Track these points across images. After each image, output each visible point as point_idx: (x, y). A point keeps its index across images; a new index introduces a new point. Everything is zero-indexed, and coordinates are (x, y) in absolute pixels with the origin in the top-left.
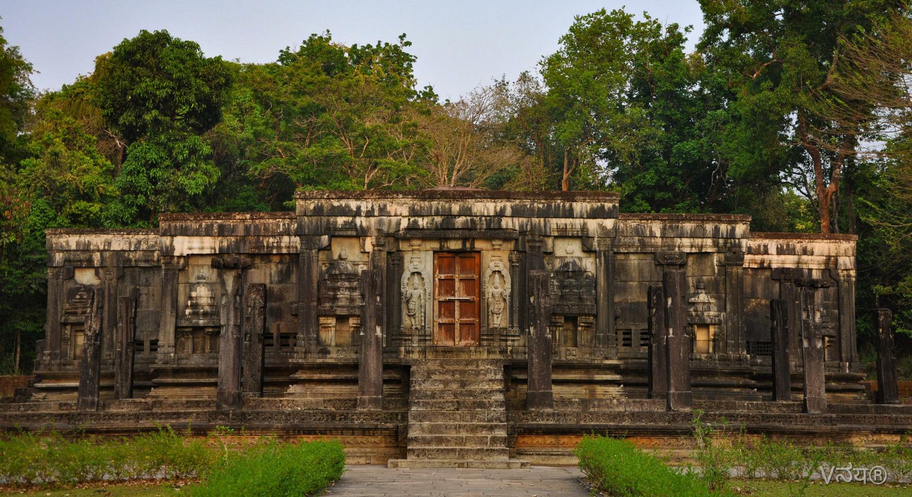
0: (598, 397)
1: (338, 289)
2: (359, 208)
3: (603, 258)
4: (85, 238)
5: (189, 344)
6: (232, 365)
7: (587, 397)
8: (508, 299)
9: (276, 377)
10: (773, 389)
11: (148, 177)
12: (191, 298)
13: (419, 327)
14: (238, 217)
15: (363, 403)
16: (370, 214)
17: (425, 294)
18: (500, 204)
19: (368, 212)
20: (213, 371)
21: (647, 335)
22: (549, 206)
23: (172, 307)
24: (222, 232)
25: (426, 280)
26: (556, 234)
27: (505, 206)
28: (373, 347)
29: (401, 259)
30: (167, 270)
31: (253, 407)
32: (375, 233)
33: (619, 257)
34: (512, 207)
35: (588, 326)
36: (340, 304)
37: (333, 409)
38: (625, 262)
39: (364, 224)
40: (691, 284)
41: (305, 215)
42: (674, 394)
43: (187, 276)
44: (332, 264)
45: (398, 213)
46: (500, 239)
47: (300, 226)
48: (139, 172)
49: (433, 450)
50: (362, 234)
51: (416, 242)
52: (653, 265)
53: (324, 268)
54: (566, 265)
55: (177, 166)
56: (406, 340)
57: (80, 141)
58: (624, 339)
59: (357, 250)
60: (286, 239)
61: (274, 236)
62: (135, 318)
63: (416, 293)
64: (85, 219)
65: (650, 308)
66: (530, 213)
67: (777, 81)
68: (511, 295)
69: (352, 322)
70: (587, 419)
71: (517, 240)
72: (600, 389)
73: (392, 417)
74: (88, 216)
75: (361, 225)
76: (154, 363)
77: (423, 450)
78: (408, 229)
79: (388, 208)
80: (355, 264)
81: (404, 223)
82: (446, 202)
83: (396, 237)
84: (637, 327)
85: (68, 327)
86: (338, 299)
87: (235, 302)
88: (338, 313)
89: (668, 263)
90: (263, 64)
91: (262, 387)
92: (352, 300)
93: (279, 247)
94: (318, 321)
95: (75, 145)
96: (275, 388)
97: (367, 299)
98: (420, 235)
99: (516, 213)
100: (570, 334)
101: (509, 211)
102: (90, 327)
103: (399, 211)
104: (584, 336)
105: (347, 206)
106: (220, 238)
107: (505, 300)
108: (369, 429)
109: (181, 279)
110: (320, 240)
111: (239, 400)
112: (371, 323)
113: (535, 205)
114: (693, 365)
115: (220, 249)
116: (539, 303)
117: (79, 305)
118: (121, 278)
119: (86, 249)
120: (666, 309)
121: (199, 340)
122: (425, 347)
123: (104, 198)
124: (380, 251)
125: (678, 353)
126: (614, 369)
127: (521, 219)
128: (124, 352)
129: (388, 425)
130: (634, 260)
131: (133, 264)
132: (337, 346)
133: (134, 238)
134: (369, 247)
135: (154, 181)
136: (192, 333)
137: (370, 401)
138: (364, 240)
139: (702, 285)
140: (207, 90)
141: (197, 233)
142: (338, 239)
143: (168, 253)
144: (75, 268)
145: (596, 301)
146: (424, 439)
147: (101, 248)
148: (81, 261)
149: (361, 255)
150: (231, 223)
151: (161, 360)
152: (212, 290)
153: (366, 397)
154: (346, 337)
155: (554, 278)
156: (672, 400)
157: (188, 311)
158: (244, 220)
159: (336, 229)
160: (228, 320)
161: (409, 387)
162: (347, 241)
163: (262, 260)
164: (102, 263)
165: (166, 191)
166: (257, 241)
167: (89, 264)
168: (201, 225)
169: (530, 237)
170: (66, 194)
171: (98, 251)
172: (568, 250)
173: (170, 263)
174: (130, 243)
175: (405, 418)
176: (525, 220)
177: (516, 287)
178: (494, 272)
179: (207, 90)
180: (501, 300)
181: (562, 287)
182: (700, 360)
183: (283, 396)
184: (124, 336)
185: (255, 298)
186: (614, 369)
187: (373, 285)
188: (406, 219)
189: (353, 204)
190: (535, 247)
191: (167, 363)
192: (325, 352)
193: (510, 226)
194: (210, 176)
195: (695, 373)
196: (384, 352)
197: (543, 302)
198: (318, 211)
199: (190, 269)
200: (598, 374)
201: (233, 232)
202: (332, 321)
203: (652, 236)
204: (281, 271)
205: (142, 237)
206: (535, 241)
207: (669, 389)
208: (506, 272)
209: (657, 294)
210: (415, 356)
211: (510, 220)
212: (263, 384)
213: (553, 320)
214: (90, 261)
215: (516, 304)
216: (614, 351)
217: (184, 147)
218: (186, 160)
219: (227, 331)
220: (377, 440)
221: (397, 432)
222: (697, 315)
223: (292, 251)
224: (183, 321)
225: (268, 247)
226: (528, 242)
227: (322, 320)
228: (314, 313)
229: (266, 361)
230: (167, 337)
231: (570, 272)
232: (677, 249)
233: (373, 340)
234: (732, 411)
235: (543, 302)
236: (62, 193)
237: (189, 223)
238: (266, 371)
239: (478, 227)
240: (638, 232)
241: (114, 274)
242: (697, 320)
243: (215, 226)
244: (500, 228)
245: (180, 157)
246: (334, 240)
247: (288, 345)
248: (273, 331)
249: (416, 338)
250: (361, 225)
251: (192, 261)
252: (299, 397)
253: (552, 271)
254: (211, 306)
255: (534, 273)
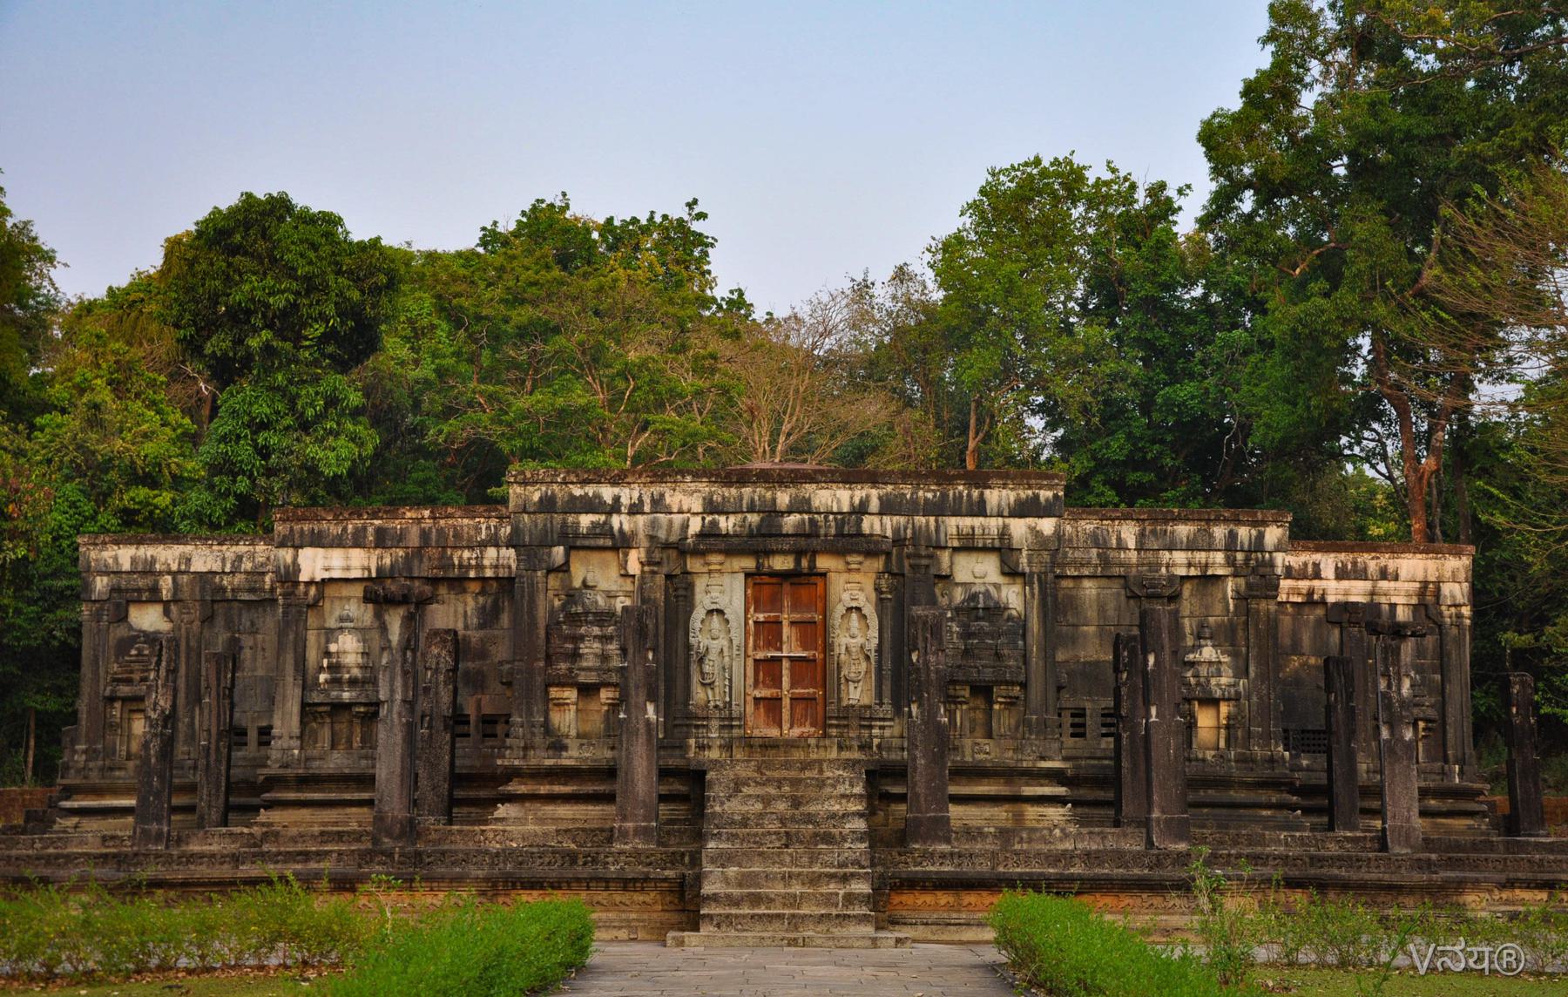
0: (1029, 824)
1: (582, 638)
2: (617, 499)
3: (1036, 586)
4: (146, 551)
5: (326, 733)
6: (398, 770)
7: (1009, 825)
8: (873, 655)
9: (474, 791)
10: (1329, 811)
11: (255, 446)
12: (328, 654)
13: (720, 704)
14: (409, 515)
15: (624, 834)
16: (635, 510)
17: (731, 647)
18: (859, 493)
19: (632, 506)
20: (366, 780)
21: (1113, 719)
22: (944, 496)
23: (296, 670)
24: (382, 540)
25: (733, 624)
26: (956, 544)
27: (868, 496)
28: (642, 739)
29: (690, 587)
30: (287, 606)
31: (434, 842)
32: (645, 543)
33: (1065, 583)
34: (880, 498)
35: (1011, 703)
36: (585, 664)
37: (573, 846)
38: (1074, 592)
39: (626, 527)
40: (1188, 630)
41: (525, 511)
42: (1158, 820)
43: (322, 616)
44: (572, 596)
45: (685, 508)
46: (859, 553)
47: (516, 531)
48: (238, 437)
49: (744, 916)
50: (621, 543)
51: (715, 559)
52: (1123, 598)
53: (557, 603)
54: (974, 597)
55: (305, 426)
56: (697, 727)
57: (138, 384)
58: (1073, 725)
59: (614, 572)
60: (491, 552)
61: (471, 548)
62: (231, 689)
63: (715, 646)
64: (145, 519)
65: (1117, 670)
66: (912, 508)
67: (1335, 280)
68: (879, 650)
69: (605, 695)
70: (1010, 862)
71: (888, 554)
72: (1031, 811)
73: (674, 860)
74: (151, 513)
75: (621, 529)
76: (265, 766)
77: (728, 916)
78: (701, 535)
79: (668, 500)
80: (610, 596)
81: (695, 525)
82: (768, 489)
83: (680, 548)
84: (1096, 704)
85: (118, 705)
86: (581, 656)
87: (405, 661)
88: (581, 679)
89: (1149, 594)
90: (452, 251)
91: (450, 808)
92: (604, 657)
93: (480, 567)
94: (547, 693)
95: (128, 391)
96: (473, 810)
97: (630, 656)
98: (723, 546)
99: (887, 508)
100: (979, 715)
101: (874, 505)
102: (156, 704)
103: (686, 504)
104: (1004, 720)
105: (597, 496)
106: (378, 551)
107: (868, 658)
108: (635, 880)
109: (312, 621)
110: (549, 554)
111: (411, 830)
112: (638, 696)
113: (921, 493)
114: (1191, 769)
115: (379, 569)
116: (926, 663)
117: (136, 666)
118: (208, 619)
119: (148, 570)
120: (1145, 673)
121: (342, 727)
122: (731, 739)
123: (178, 482)
124: (653, 573)
125: (1165, 749)
126: (1056, 776)
127: (895, 518)
128: (213, 747)
129: (667, 873)
130: (1090, 589)
131: (229, 595)
132: (579, 736)
133: (230, 551)
134: (634, 567)
135: (264, 452)
136: (330, 714)
137: (637, 832)
138: (626, 555)
139: (1207, 632)
140: (355, 295)
141: (338, 543)
142: (582, 553)
143: (289, 577)
144: (128, 602)
145: (1025, 658)
146: (728, 897)
147: (174, 567)
148: (139, 590)
149: (621, 580)
150: (397, 525)
151: (276, 761)
152: (365, 641)
153: (630, 825)
154: (596, 722)
155: (952, 619)
156: (1155, 829)
157: (323, 677)
158: (419, 520)
159: (577, 535)
160: (392, 691)
161: (702, 806)
162: (595, 557)
163: (451, 588)
164: (175, 594)
165: (286, 470)
166: (443, 556)
167: (154, 596)
168: (345, 529)
169: (911, 549)
170: (113, 475)
171: (169, 572)
172: (977, 572)
173: (293, 593)
174: (224, 560)
175: (696, 860)
176: (902, 520)
177: (888, 635)
178: (850, 609)
179: (355, 295)
180: (862, 657)
181: (966, 635)
182: (1204, 760)
183: (486, 822)
184: (214, 720)
185: (439, 654)
186: (1056, 776)
187: (642, 632)
188: (699, 518)
189: (607, 493)
190: (919, 566)
191: (286, 766)
192: (558, 747)
193: (877, 530)
194: (361, 445)
195: (1194, 783)
196: (661, 747)
197: (933, 661)
198: (547, 504)
199: (327, 605)
200: (1028, 785)
201: (400, 540)
202: (571, 694)
203: (1121, 547)
204: (484, 607)
205: (245, 549)
206: (920, 556)
207: (1149, 811)
208: (869, 610)
209: (1129, 647)
210: (714, 754)
211: (876, 519)
212: (453, 802)
213: (951, 692)
214: (155, 590)
215: (887, 665)
216: (1056, 745)
217: (317, 393)
218: (321, 417)
219: (390, 711)
220: (647, 899)
221: (682, 885)
222: (1198, 684)
223: (502, 573)
224: (314, 694)
225: (461, 566)
226: (909, 557)
227: (554, 692)
228: (539, 679)
229: (458, 762)
230: (286, 721)
231: (981, 611)
232: (1163, 570)
233: (641, 726)
234: (1259, 849)
235: (933, 661)
236: (107, 473)
237: (325, 525)
238: (457, 779)
239: (822, 532)
240: (1097, 540)
241: (196, 612)
242: (1198, 692)
243: (370, 530)
244: (860, 534)
245: (310, 412)
246: (573, 554)
247: (495, 736)
248: (470, 710)
249: (715, 724)
250: (621, 529)
251: (330, 591)
252: (515, 825)
253: (949, 607)
254: (363, 667)
255: (918, 611)
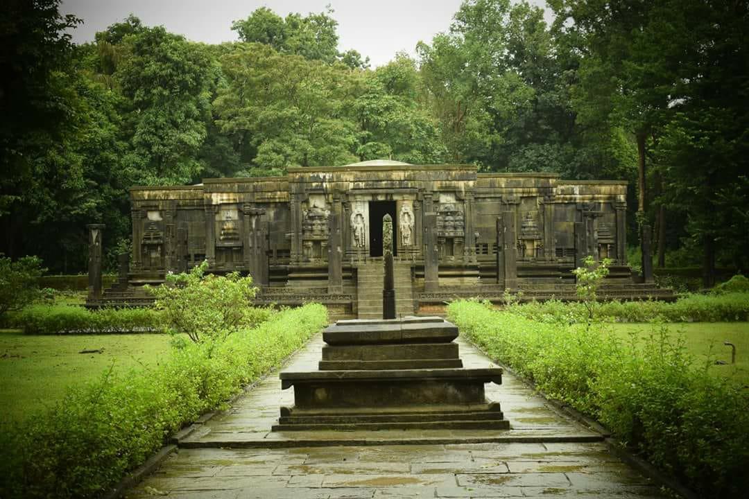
2: (324, 177)
12: (223, 229)
36: (315, 233)
75: (326, 188)
81: (351, 186)
162: (317, 197)
223: (282, 200)
250: (326, 188)
